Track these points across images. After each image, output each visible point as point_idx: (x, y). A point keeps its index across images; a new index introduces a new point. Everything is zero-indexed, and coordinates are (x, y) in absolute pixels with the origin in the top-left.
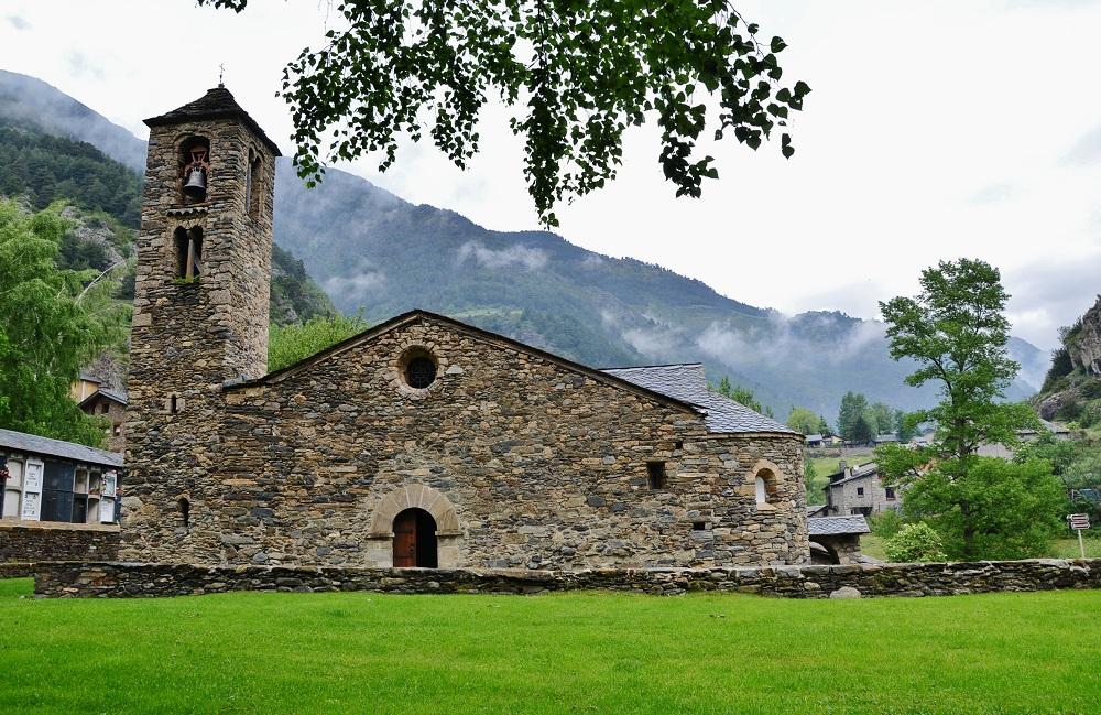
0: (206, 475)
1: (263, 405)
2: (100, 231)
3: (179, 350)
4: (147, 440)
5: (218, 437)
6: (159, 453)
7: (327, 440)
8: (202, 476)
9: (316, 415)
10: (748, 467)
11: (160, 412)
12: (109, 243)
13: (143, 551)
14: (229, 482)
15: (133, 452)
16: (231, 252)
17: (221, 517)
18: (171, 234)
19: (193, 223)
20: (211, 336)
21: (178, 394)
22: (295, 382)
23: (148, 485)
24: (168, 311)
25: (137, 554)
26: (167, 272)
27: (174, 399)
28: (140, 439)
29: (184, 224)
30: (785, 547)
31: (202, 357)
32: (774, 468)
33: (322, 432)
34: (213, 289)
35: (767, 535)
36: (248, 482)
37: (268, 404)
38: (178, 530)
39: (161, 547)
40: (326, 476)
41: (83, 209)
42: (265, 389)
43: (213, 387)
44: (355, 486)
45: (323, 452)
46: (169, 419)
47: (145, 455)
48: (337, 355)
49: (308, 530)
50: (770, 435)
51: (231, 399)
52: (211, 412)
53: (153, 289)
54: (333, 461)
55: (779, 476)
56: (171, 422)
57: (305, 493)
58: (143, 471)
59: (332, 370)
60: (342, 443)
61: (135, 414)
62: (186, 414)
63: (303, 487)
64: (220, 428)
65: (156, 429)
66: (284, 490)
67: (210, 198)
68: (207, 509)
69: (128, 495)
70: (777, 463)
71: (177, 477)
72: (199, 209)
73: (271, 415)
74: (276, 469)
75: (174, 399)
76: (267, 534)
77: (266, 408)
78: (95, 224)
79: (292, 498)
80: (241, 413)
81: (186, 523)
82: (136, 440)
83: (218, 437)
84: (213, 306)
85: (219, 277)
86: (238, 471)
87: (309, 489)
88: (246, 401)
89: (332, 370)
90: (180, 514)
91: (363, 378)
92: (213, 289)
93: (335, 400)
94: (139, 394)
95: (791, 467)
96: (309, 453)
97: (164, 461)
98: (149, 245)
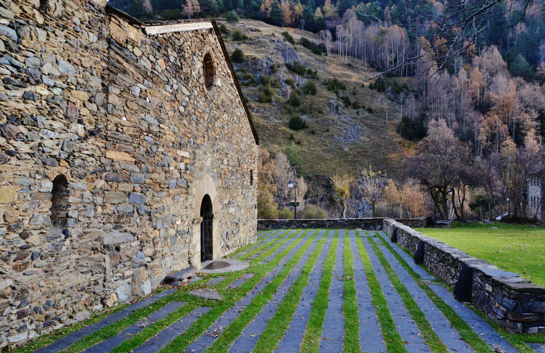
0: (86, 138)
14: (111, 154)
17: (103, 206)
68: (88, 194)
80: (123, 58)
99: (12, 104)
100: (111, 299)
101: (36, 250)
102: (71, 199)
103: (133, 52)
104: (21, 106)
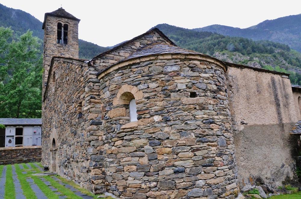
2: (225, 56)
10: (114, 95)
12: (227, 58)
16: (47, 58)
30: (145, 161)
32: (134, 91)
35: (127, 150)
41: (220, 51)
50: (127, 64)
55: (139, 96)
70: (136, 85)
78: (224, 54)
95: (153, 85)
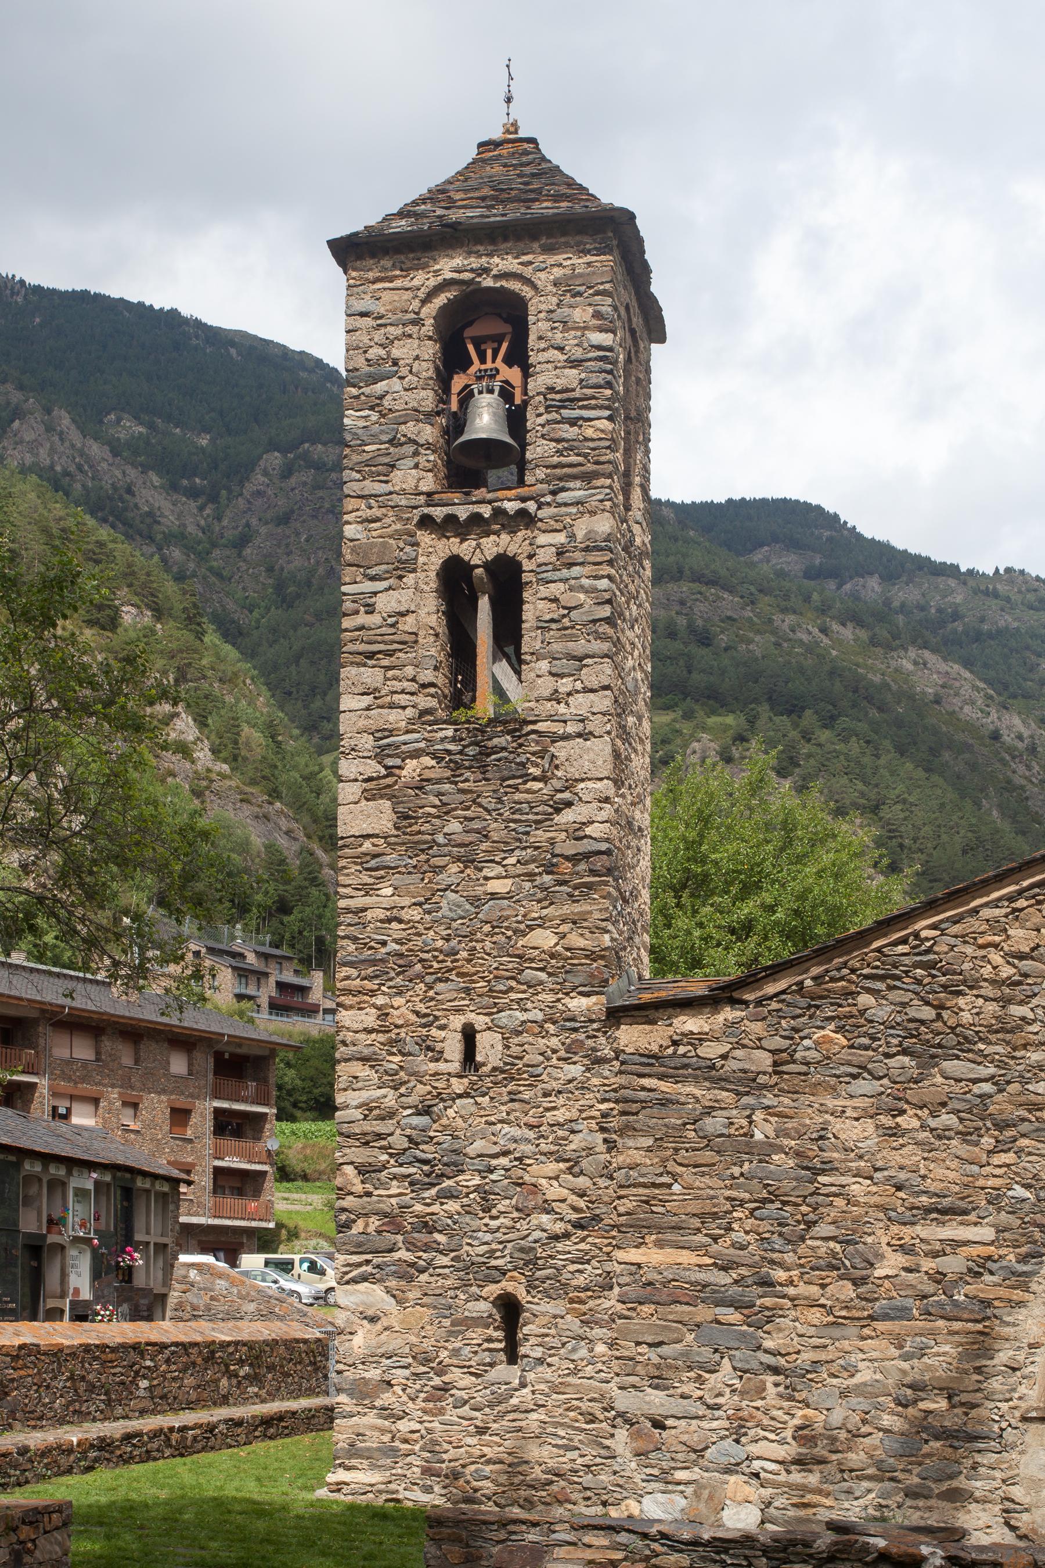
0: (567, 1235)
1: (724, 1057)
3: (475, 901)
4: (399, 1141)
5: (599, 1137)
6: (436, 1172)
7: (911, 1155)
8: (556, 1238)
9: (875, 1086)
11: (432, 1067)
13: (404, 1426)
15: (364, 1170)
18: (427, 578)
19: (492, 546)
20: (566, 867)
21: (481, 1021)
22: (814, 1000)
23: (403, 1254)
24: (439, 794)
25: (383, 1431)
26: (424, 686)
27: (469, 1035)
28: (380, 1136)
29: (465, 549)
31: (542, 923)
33: (894, 1132)
34: (566, 737)
36: (686, 1257)
37: (738, 1053)
38: (493, 1374)
39: (452, 1415)
40: (906, 1250)
42: (728, 1014)
43: (578, 1004)
44: (987, 1278)
45: (899, 1188)
46: (458, 1086)
47: (395, 1177)
48: (934, 927)
49: (860, 1390)
51: (631, 1037)
52: (575, 1070)
53: (391, 732)
54: (928, 1210)
56: (466, 1095)
57: (848, 1291)
58: (392, 1221)
59: (917, 965)
60: (954, 1164)
61: (363, 1071)
62: (506, 1073)
63: (841, 1278)
64: (605, 1115)
65: (425, 1111)
66: (791, 1283)
67: (541, 473)
69: (354, 1281)
71: (488, 1237)
72: (511, 507)
73: (747, 1083)
74: (765, 1226)
75: (469, 1035)
76: (743, 1393)
77: (732, 1065)
79: (814, 1304)
80: (662, 1077)
81: (512, 1356)
82: (366, 1141)
83: (599, 1137)
84: (570, 784)
85: (581, 704)
86: (660, 1229)
87: (856, 1282)
88: (675, 1043)
89: (917, 965)
90: (500, 1334)
91: (1010, 991)
92: (566, 737)
93: (926, 1046)
94: (369, 1018)
96: (858, 1188)
97: (449, 1195)
98: (370, 609)
99: (418, 1208)
100: (623, 1508)
101: (463, 1394)
102: (526, 1330)
103: (697, 1056)
104: (436, 1208)
